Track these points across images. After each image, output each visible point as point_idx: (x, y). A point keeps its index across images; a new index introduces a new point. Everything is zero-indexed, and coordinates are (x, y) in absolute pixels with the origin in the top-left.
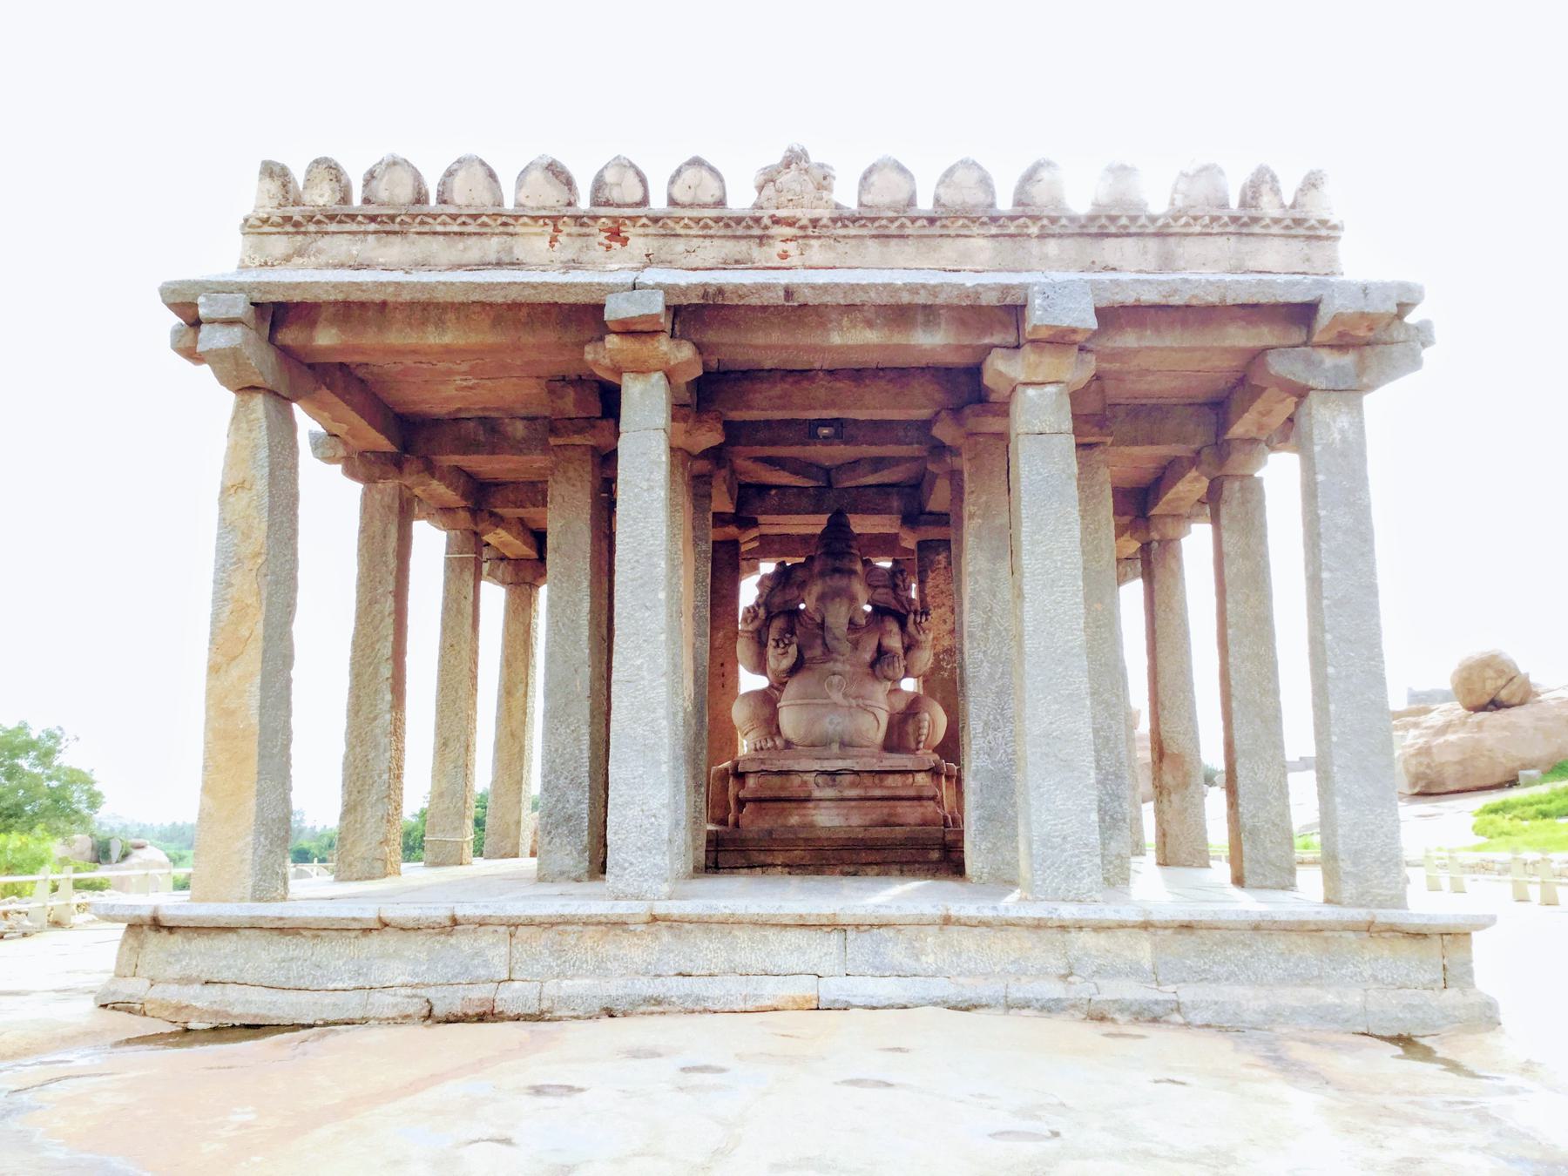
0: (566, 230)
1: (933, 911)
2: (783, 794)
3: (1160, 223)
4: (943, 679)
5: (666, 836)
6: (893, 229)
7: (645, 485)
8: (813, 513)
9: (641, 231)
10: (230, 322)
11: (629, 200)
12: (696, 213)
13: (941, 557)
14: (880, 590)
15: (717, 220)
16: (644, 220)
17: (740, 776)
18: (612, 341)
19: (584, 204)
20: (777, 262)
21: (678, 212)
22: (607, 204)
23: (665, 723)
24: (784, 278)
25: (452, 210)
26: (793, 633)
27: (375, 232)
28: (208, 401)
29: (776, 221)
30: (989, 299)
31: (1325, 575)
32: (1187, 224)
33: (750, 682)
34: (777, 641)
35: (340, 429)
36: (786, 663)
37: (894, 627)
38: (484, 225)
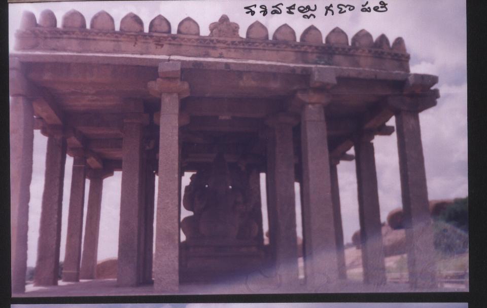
6: (261, 47)
7: (170, 134)
11: (163, 31)
12: (190, 37)
15: (197, 40)
18: (159, 80)
22: (156, 32)
24: (225, 60)
25: (96, 31)
29: (219, 42)
30: (298, 72)
33: (185, 213)
35: (44, 115)
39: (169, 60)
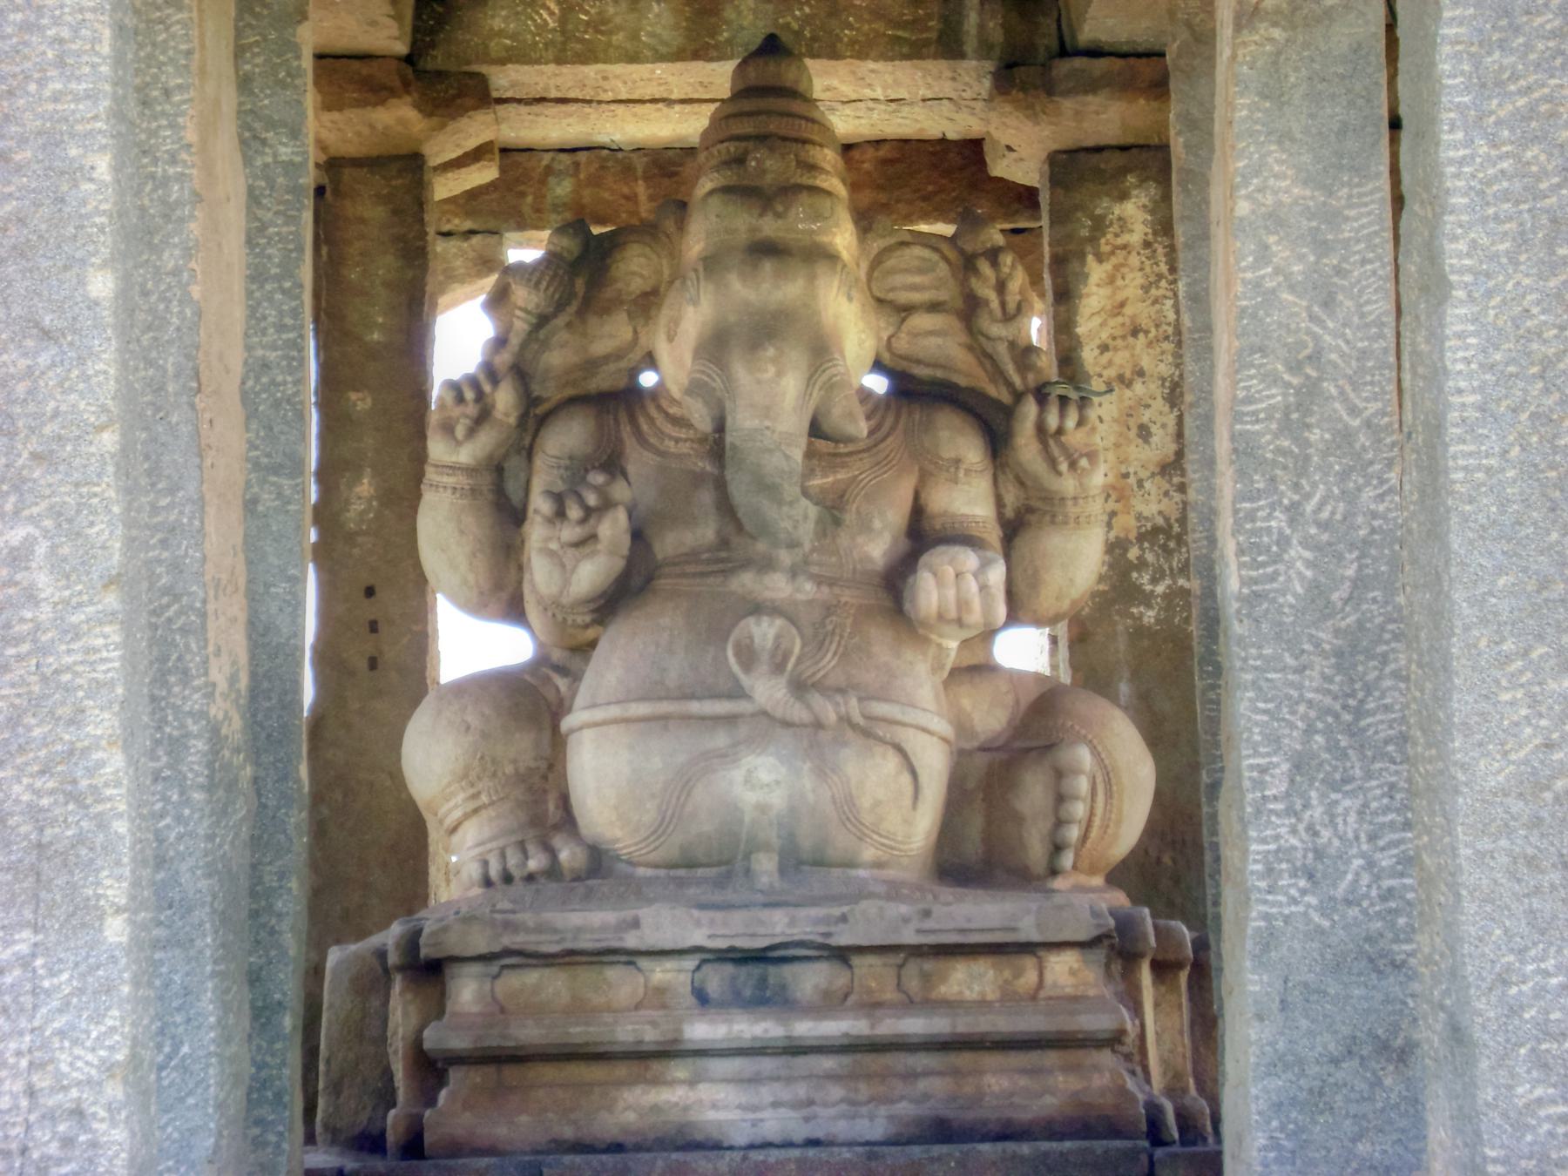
2: (578, 1033)
4: (1139, 632)
8: (678, 56)
13: (1133, 212)
14: (922, 321)
17: (429, 971)
23: (115, 761)
26: (612, 464)
34: (559, 500)
36: (590, 574)
37: (969, 449)
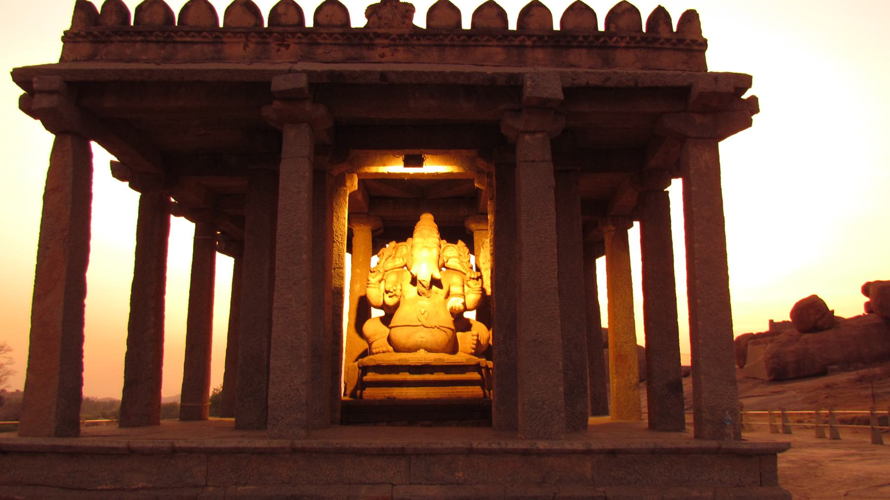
0: (254, 40)
1: (463, 446)
3: (602, 40)
5: (304, 401)
9: (297, 41)
10: (51, 92)
15: (342, 34)
16: (300, 35)
18: (277, 104)
19: (266, 25)
20: (378, 59)
21: (322, 30)
22: (279, 25)
24: (379, 68)
27: (141, 41)
28: (39, 140)
29: (378, 36)
31: (696, 245)
32: (617, 41)
38: (205, 37)
39: (290, 71)
